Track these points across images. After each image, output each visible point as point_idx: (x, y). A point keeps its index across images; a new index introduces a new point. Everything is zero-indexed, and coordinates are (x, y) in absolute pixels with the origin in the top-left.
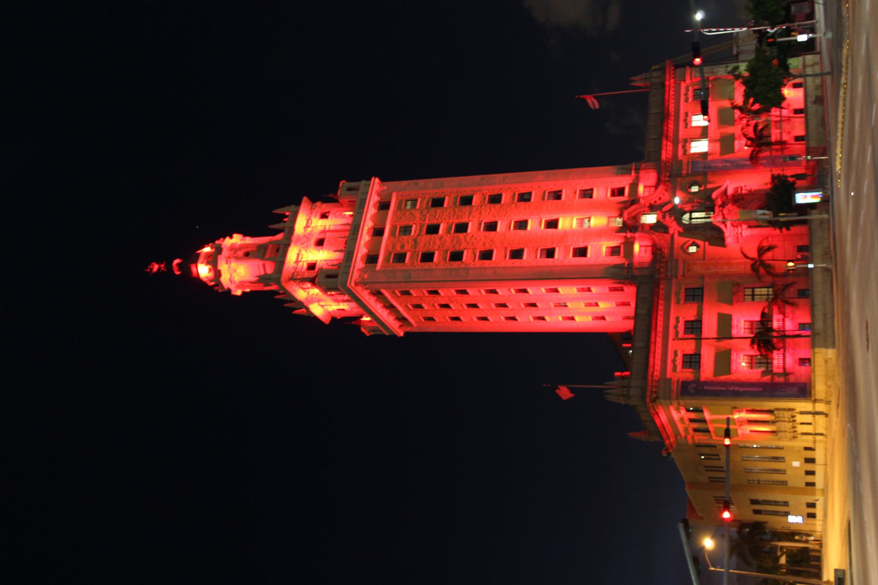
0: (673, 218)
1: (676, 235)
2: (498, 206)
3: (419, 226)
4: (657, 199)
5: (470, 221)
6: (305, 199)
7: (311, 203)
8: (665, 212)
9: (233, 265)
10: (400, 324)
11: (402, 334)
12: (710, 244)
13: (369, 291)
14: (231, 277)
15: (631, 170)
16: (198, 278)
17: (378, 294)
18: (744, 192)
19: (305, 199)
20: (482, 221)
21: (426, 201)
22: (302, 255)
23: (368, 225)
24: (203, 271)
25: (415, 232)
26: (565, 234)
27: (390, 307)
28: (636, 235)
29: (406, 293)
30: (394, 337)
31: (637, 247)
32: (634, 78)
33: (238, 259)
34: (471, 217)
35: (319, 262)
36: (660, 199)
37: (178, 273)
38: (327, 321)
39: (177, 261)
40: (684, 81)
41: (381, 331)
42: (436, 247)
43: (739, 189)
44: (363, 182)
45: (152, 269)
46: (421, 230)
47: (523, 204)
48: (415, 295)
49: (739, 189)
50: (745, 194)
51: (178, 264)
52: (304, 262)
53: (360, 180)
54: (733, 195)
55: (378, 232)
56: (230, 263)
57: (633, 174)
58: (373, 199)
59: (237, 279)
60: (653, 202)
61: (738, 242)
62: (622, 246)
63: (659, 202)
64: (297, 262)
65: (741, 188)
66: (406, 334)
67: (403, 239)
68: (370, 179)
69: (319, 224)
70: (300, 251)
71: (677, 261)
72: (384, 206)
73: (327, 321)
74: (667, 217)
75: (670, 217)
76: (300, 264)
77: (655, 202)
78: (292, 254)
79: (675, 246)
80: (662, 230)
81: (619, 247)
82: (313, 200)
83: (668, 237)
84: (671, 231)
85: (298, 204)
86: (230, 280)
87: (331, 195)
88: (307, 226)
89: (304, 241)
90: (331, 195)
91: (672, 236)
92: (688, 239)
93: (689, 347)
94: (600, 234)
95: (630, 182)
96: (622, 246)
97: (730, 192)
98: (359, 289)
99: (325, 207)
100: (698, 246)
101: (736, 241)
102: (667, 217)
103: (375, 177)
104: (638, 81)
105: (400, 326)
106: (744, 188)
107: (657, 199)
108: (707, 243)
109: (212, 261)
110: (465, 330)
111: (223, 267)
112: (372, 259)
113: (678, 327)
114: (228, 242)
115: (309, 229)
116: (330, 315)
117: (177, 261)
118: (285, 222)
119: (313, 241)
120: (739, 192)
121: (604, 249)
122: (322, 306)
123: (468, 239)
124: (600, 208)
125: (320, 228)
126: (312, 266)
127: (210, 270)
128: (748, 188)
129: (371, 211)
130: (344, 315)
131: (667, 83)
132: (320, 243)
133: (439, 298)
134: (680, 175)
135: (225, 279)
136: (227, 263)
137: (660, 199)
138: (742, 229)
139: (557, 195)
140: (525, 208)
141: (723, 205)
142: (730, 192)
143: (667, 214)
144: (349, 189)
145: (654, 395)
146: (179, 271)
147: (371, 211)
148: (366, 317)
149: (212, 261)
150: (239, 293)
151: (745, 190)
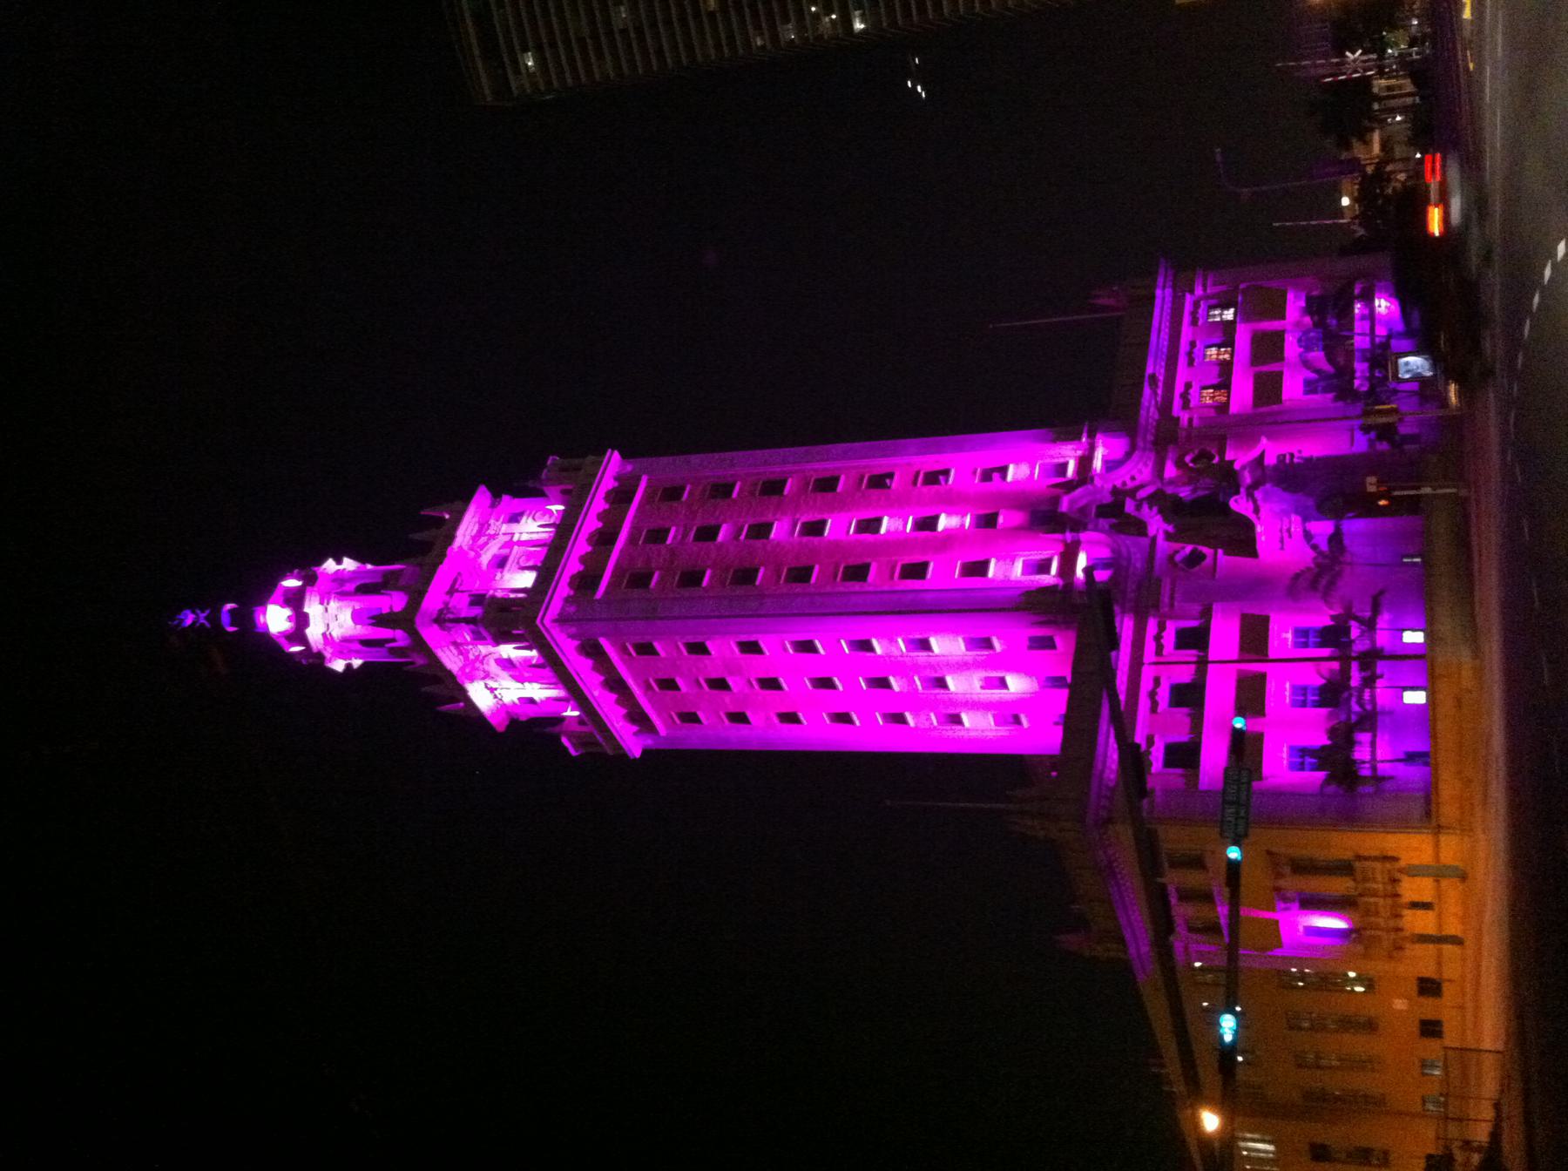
0: (1155, 509)
1: (1160, 538)
2: (830, 495)
3: (681, 529)
5: (776, 520)
8: (1142, 500)
9: (333, 605)
11: (637, 754)
12: (1226, 553)
13: (577, 643)
14: (328, 629)
16: (264, 633)
17: (592, 650)
18: (1295, 460)
20: (798, 520)
22: (462, 581)
24: (276, 619)
25: (674, 538)
27: (615, 684)
28: (1083, 536)
29: (646, 649)
30: (622, 757)
33: (343, 596)
34: (778, 516)
36: (1133, 478)
37: (231, 629)
38: (500, 725)
39: (229, 606)
40: (1192, 292)
41: (600, 745)
42: (709, 563)
43: (1287, 456)
44: (591, 458)
45: (182, 621)
46: (685, 536)
47: (875, 492)
48: (662, 654)
49: (1287, 456)
50: (1299, 464)
51: (231, 611)
53: (584, 456)
54: (1276, 468)
56: (328, 604)
59: (337, 633)
60: (1118, 484)
61: (1282, 548)
63: (1130, 485)
65: (1292, 455)
66: (645, 752)
67: (651, 549)
68: (603, 453)
72: (621, 496)
73: (500, 725)
74: (1145, 509)
75: (1150, 508)
77: (1124, 484)
83: (1145, 541)
84: (1151, 531)
85: (466, 499)
86: (324, 635)
87: (530, 484)
90: (530, 484)
91: (1154, 539)
92: (1182, 545)
97: (1270, 460)
101: (1280, 546)
102: (1145, 509)
103: (613, 450)
106: (1296, 455)
108: (1220, 551)
109: (294, 601)
110: (755, 746)
111: (313, 608)
113: (1156, 694)
114: (330, 566)
117: (229, 606)
120: (1288, 461)
122: (492, 690)
123: (769, 548)
127: (290, 619)
128: (1305, 454)
129: (597, 504)
130: (531, 713)
131: (1158, 292)
133: (707, 662)
135: (314, 633)
136: (322, 603)
137: (1133, 478)
138: (1290, 523)
141: (1255, 485)
142: (1270, 460)
143: (1145, 502)
144: (563, 470)
145: (1104, 814)
146: (232, 625)
147: (597, 504)
148: (572, 710)
149: (294, 601)
150: (339, 665)
151: (1298, 458)
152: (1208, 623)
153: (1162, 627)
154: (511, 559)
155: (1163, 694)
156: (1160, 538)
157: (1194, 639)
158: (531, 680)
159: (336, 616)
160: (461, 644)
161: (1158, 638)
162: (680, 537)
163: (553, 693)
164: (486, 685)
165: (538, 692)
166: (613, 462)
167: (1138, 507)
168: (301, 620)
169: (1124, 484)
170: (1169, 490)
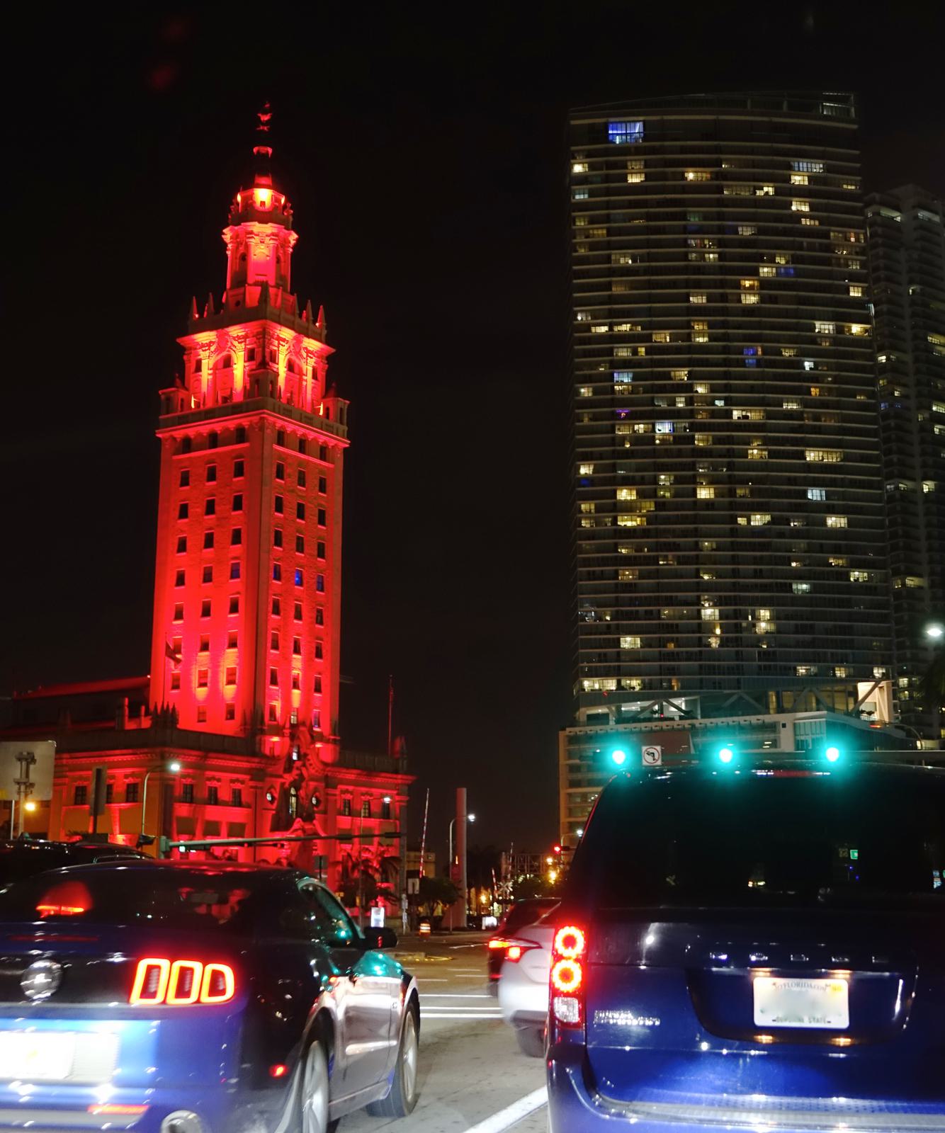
0: (297, 777)
1: (282, 780)
2: (315, 587)
4: (311, 762)
6: (333, 350)
7: (325, 355)
8: (301, 770)
10: (178, 440)
15: (335, 735)
19: (333, 350)
21: (323, 503)
23: (312, 434)
26: (289, 661)
27: (213, 440)
28: (287, 740)
31: (276, 739)
32: (403, 740)
33: (276, 249)
35: (276, 366)
36: (311, 765)
37: (255, 150)
39: (270, 150)
52: (278, 347)
53: (347, 425)
55: (302, 446)
57: (332, 737)
58: (332, 443)
59: (254, 241)
60: (309, 757)
62: (275, 723)
64: (279, 339)
68: (348, 438)
69: (308, 366)
70: (288, 342)
71: (262, 780)
72: (323, 453)
74: (298, 772)
75: (297, 775)
76: (276, 343)
77: (309, 760)
78: (287, 333)
79: (274, 779)
80: (287, 767)
81: (275, 720)
82: (330, 359)
83: (281, 772)
84: (286, 776)
85: (327, 341)
86: (252, 233)
88: (308, 352)
89: (296, 349)
91: (281, 777)
93: (225, 794)
94: (287, 700)
95: (325, 734)
96: (275, 723)
98: (256, 419)
99: (322, 375)
100: (272, 802)
104: (399, 743)
105: (175, 439)
107: (311, 762)
108: (274, 812)
111: (269, 228)
112: (281, 438)
115: (305, 355)
116: (191, 349)
118: (300, 316)
119: (294, 358)
120: (314, 848)
121: (274, 703)
124: (306, 700)
125: (304, 367)
126: (274, 358)
130: (191, 367)
131: (400, 776)
132: (291, 366)
134: (327, 787)
136: (273, 234)
139: (319, 654)
140: (311, 618)
144: (341, 409)
146: (258, 152)
150: (228, 235)
152: (244, 807)
153: (243, 782)
154: (292, 374)
155: (215, 784)
156: (282, 780)
157: (237, 801)
158: (214, 374)
159: (263, 242)
160: (245, 341)
161: (237, 780)
162: (300, 494)
163: (204, 387)
164: (213, 343)
165: (206, 374)
166: (346, 443)
167: (298, 768)
168: (264, 217)
169: (309, 760)
170: (304, 784)
